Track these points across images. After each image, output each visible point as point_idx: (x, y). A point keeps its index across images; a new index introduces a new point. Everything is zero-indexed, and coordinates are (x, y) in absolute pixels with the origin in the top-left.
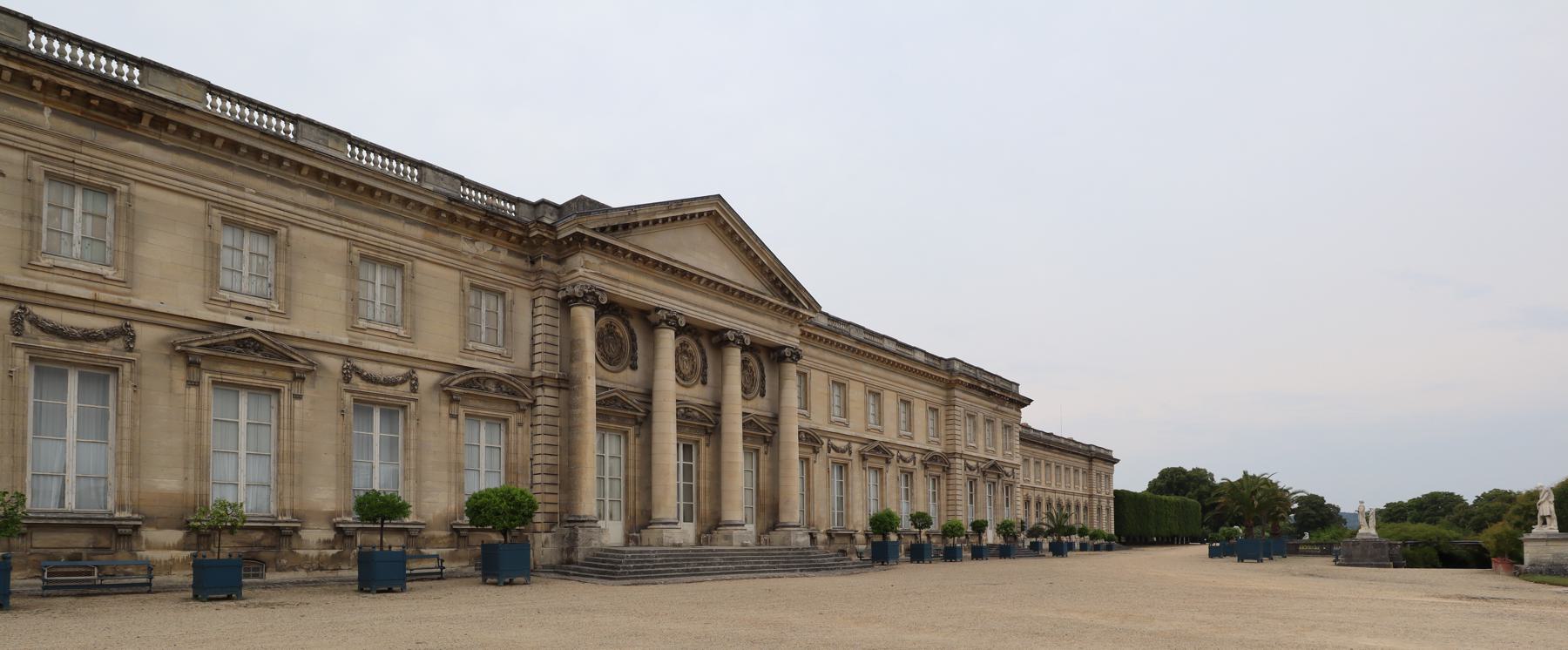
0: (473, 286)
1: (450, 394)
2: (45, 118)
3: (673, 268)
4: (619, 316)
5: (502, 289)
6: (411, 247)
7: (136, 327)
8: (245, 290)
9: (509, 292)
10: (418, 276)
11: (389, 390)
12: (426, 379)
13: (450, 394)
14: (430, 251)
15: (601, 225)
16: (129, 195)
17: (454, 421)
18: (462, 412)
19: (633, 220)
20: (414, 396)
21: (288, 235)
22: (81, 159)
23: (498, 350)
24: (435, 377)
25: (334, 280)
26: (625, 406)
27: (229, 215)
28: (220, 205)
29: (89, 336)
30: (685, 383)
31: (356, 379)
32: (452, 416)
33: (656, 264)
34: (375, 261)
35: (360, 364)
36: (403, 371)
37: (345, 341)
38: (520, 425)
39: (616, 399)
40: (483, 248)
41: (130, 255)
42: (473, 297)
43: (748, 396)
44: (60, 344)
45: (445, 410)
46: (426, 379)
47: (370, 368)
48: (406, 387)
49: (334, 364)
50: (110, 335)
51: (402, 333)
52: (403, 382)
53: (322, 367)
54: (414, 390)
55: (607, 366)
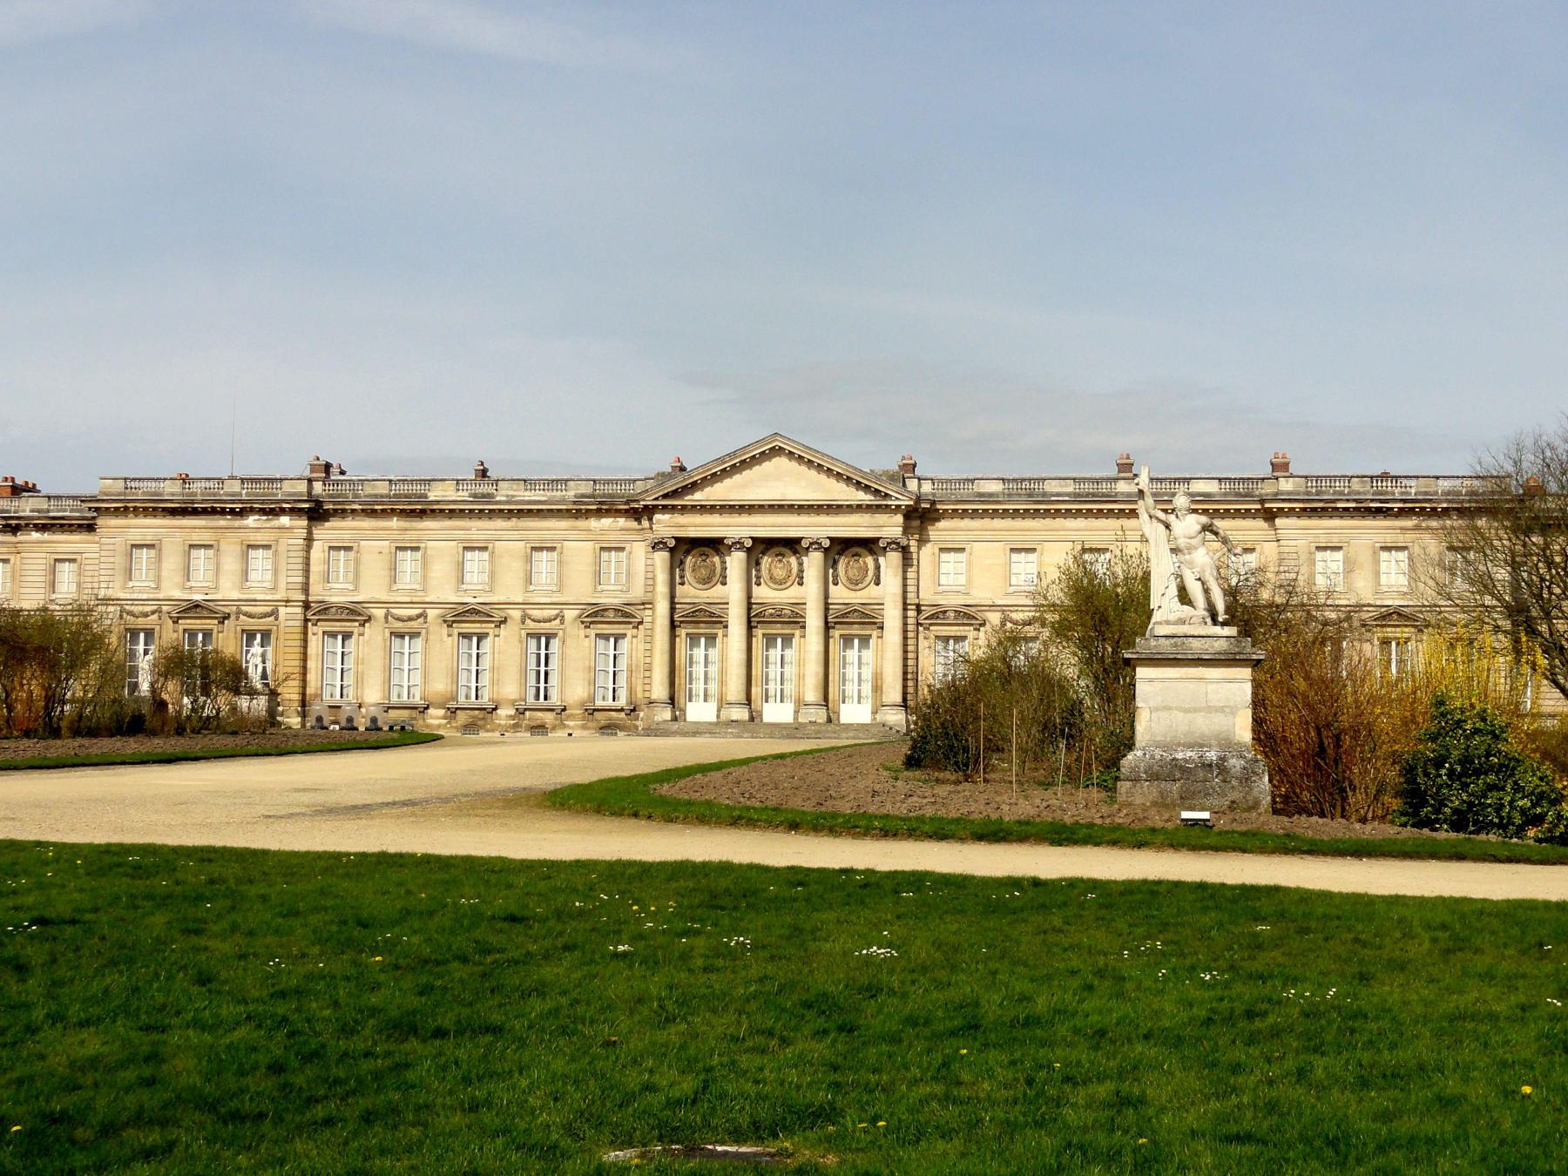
0: (602, 549)
1: (583, 622)
2: (395, 522)
3: (730, 506)
4: (708, 546)
5: (623, 545)
6: (559, 535)
7: (428, 610)
8: (476, 581)
9: (628, 546)
10: (565, 551)
11: (547, 625)
12: (570, 614)
13: (583, 622)
14: (573, 535)
15: (661, 493)
16: (426, 548)
17: (587, 639)
18: (592, 632)
19: (691, 481)
20: (562, 627)
21: (494, 547)
22: (407, 537)
23: (620, 588)
24: (577, 612)
25: (518, 566)
26: (712, 614)
27: (466, 545)
28: (461, 541)
29: (410, 619)
30: (784, 586)
31: (528, 621)
32: (586, 637)
33: (713, 507)
34: (541, 549)
35: (530, 612)
36: (556, 612)
37: (521, 601)
38: (633, 637)
39: (701, 610)
40: (607, 522)
41: (425, 577)
42: (605, 555)
43: (860, 586)
44: (400, 624)
45: (582, 632)
46: (570, 614)
47: (536, 613)
48: (558, 621)
49: (516, 614)
50: (419, 616)
51: (555, 589)
52: (555, 619)
53: (511, 617)
54: (562, 624)
55: (700, 586)
